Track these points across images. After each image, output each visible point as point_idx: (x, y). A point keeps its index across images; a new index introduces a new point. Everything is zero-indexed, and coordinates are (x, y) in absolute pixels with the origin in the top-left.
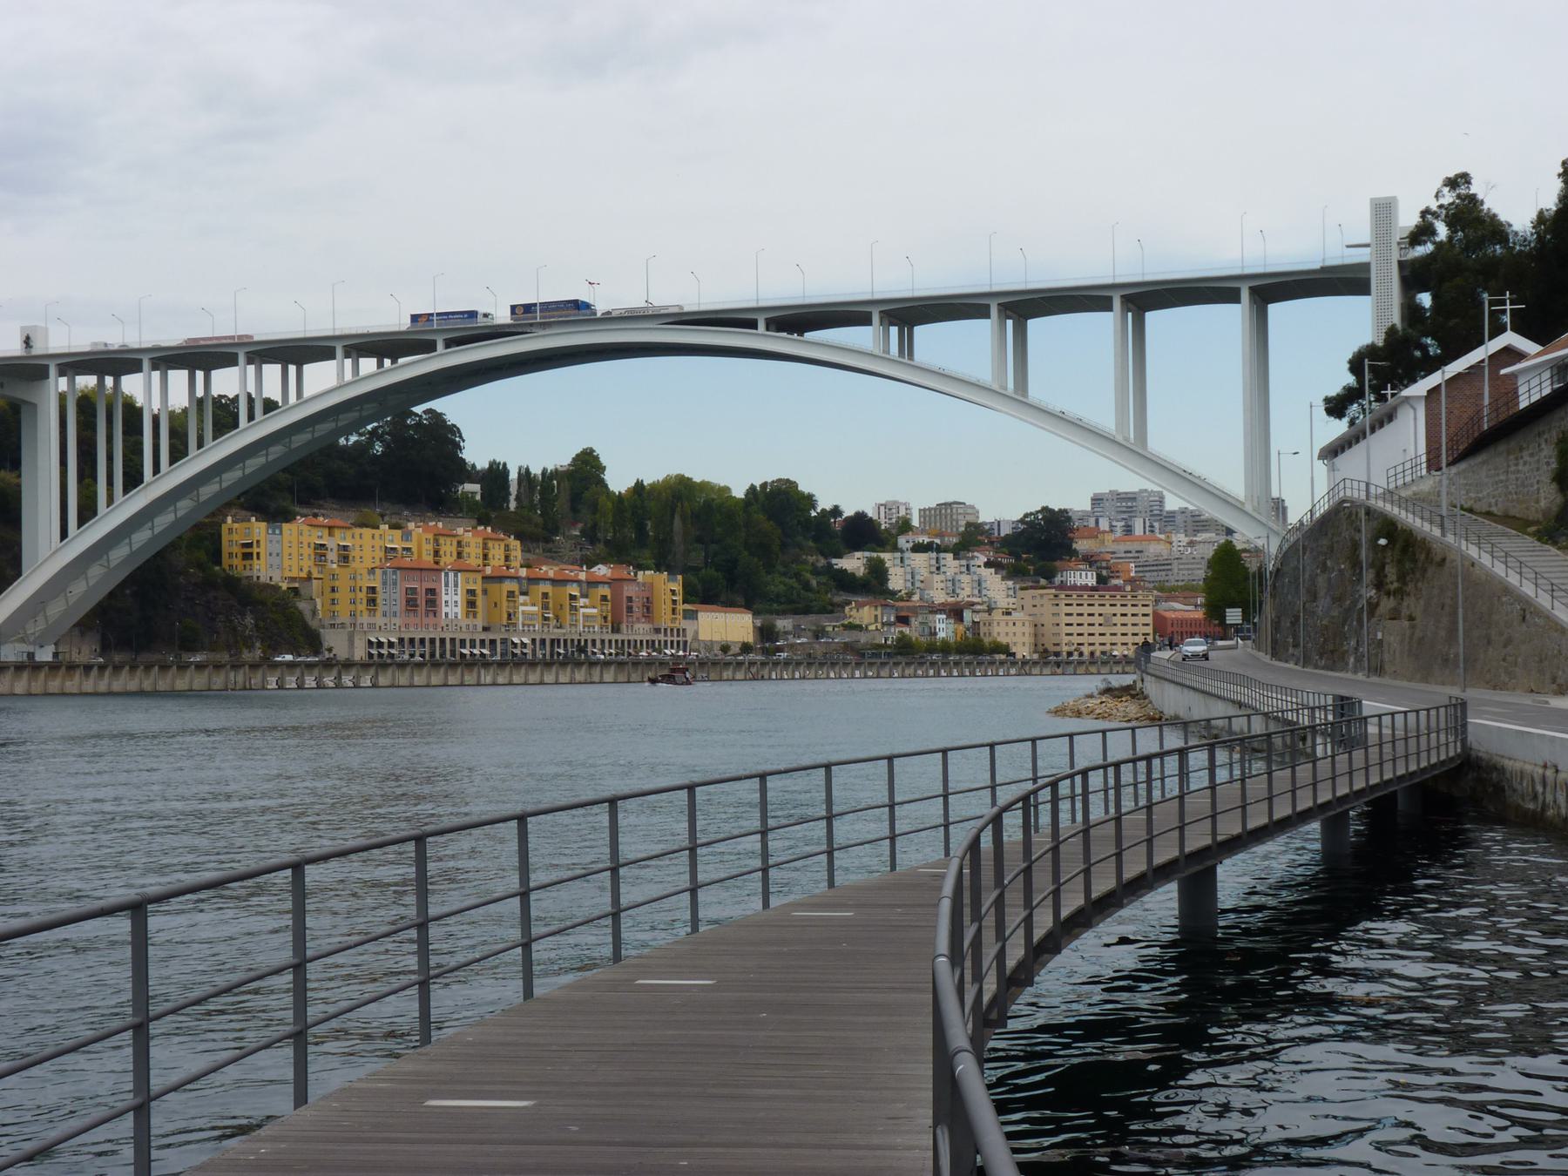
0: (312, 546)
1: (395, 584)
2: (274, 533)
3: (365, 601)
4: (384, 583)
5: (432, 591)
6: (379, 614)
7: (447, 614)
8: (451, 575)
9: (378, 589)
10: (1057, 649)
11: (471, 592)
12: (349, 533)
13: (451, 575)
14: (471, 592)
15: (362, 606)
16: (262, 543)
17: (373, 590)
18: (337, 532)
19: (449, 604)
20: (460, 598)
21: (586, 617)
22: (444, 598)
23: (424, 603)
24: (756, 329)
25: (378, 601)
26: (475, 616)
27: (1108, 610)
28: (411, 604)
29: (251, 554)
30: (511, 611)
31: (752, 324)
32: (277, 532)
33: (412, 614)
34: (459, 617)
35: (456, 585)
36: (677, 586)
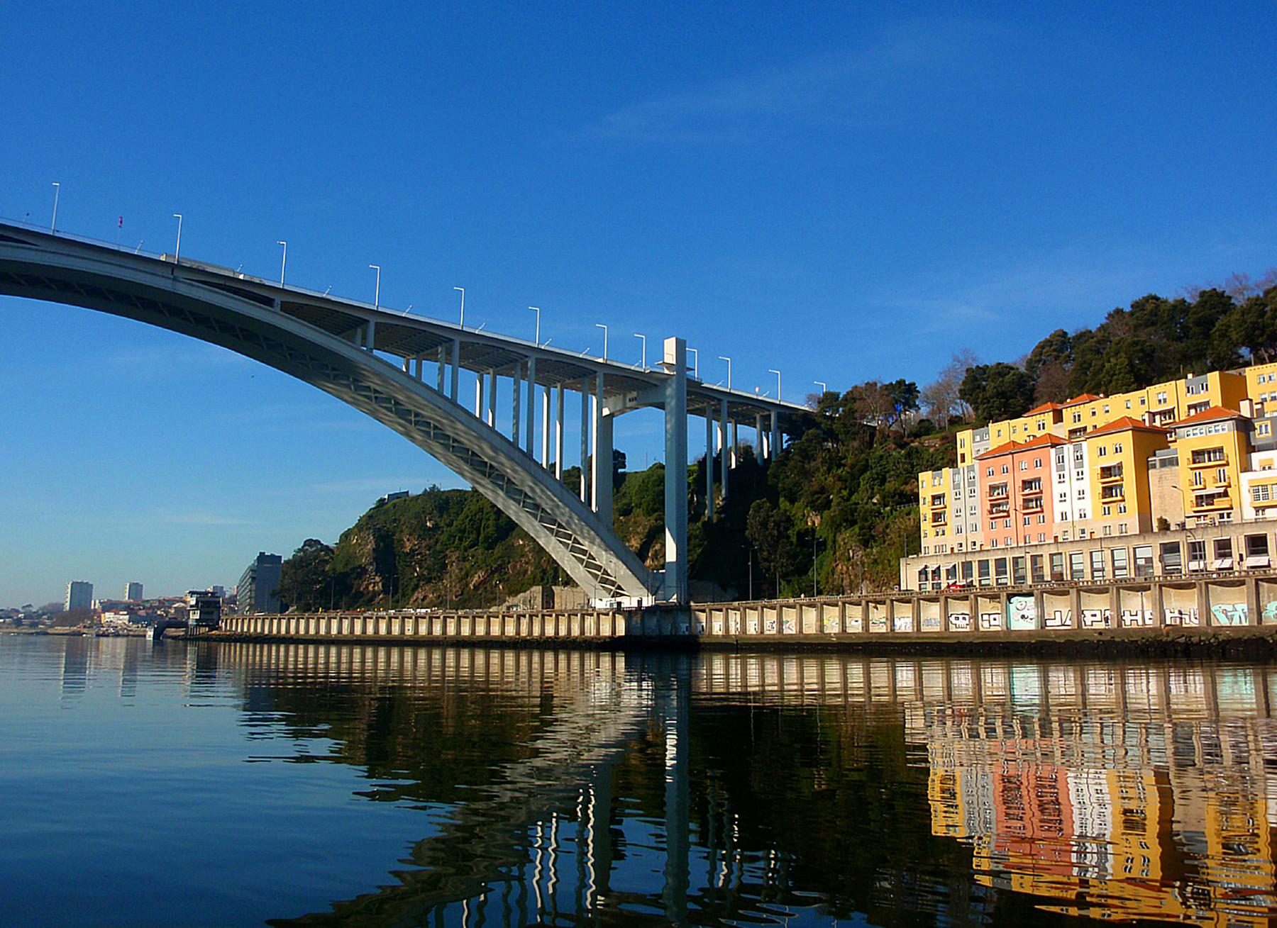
7: (1064, 516)
12: (1085, 410)
18: (1067, 414)
20: (1092, 484)
22: (1058, 489)
28: (997, 508)
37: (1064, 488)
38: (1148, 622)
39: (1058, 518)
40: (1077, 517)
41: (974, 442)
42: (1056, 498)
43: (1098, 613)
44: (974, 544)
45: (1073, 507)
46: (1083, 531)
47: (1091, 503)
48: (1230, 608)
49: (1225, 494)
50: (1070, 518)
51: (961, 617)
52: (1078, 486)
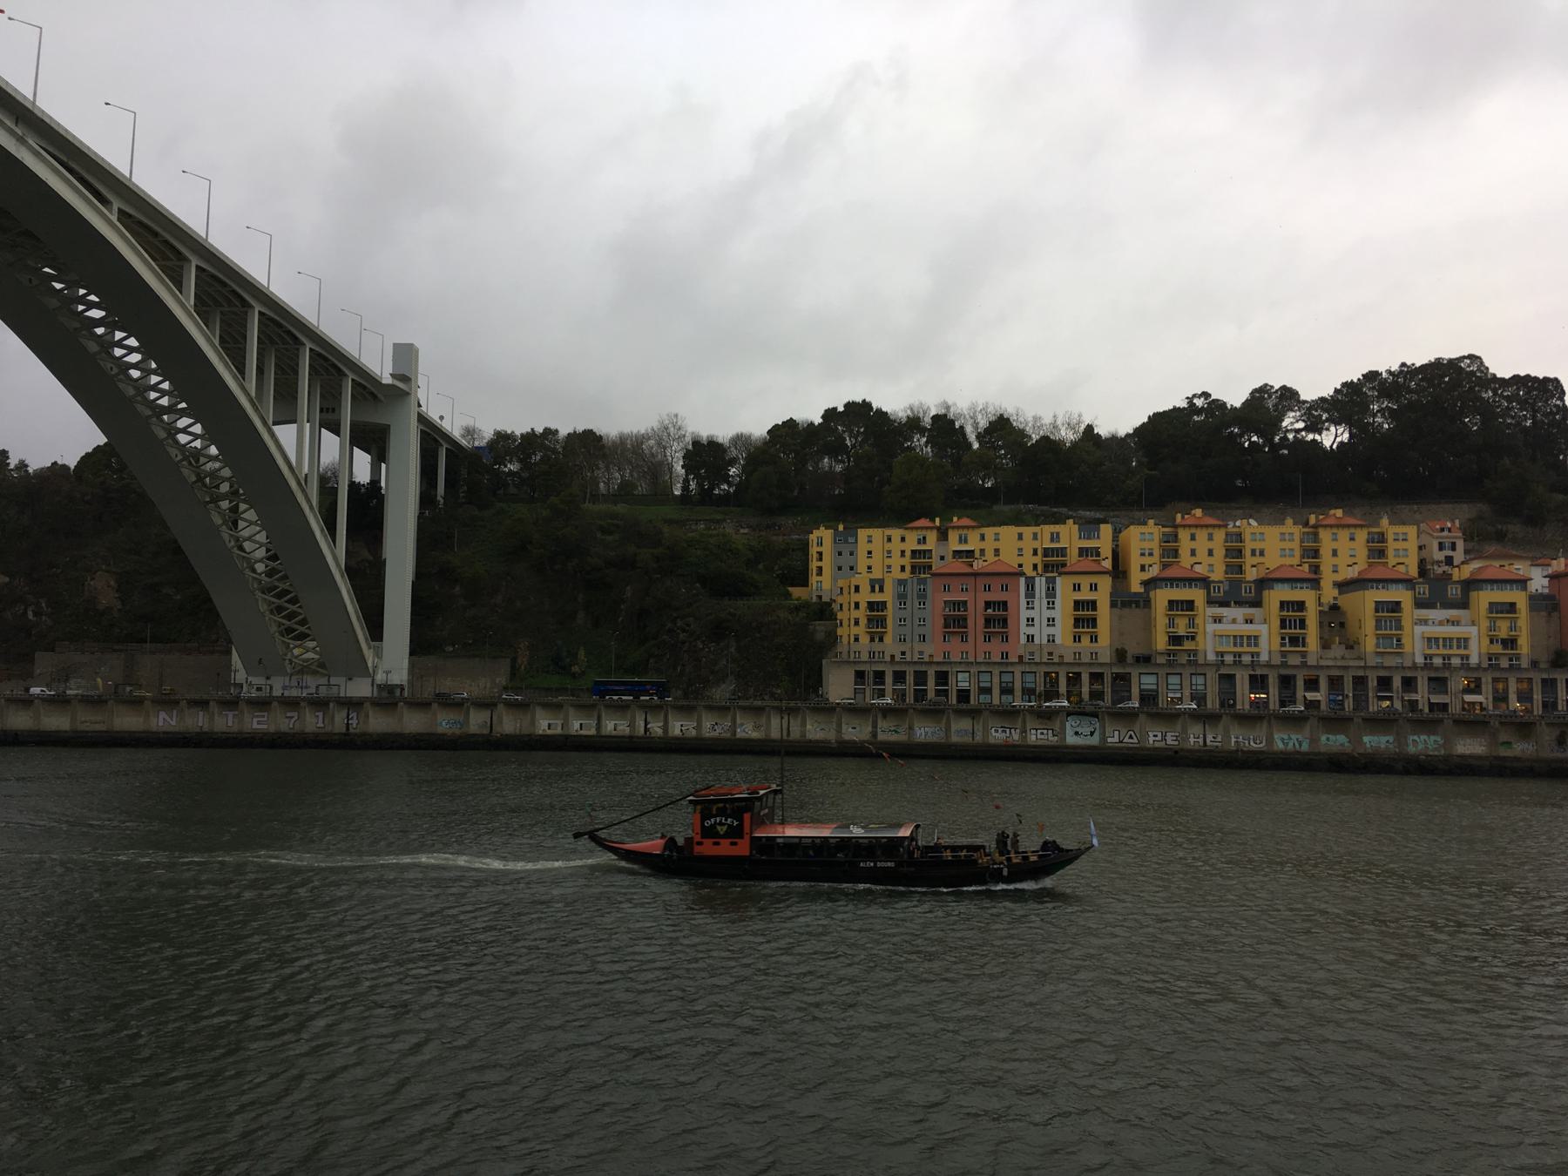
0: (908, 554)
1: (922, 596)
2: (846, 542)
3: (863, 622)
4: (902, 598)
6: (888, 639)
7: (1030, 638)
8: (1040, 584)
9: (889, 606)
11: (1093, 605)
13: (1040, 584)
18: (953, 536)
19: (1036, 621)
21: (1431, 641)
22: (1024, 614)
23: (981, 622)
25: (889, 622)
26: (1094, 639)
28: (955, 622)
30: (1181, 632)
32: (851, 540)
33: (956, 640)
34: (1058, 641)
35: (1051, 593)
37: (1031, 614)
38: (1208, 742)
39: (1023, 640)
40: (1045, 641)
41: (835, 542)
42: (1023, 622)
43: (1160, 734)
44: (921, 653)
45: (1041, 633)
46: (1050, 654)
47: (1063, 632)
48: (1286, 737)
49: (1193, 638)
50: (1037, 640)
51: (1000, 730)
52: (1048, 614)
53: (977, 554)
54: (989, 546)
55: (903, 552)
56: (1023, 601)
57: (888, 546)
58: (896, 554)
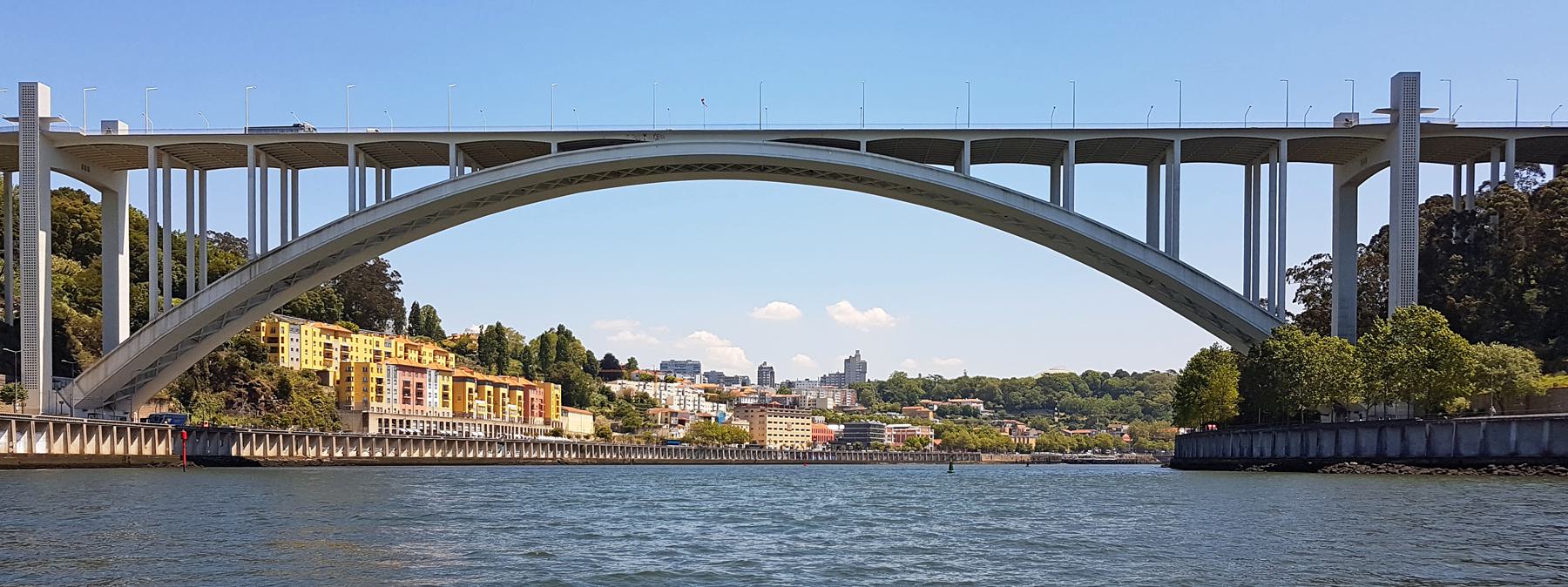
0: (322, 345)
5: (419, 385)
10: (763, 444)
14: (445, 387)
15: (373, 394)
16: (285, 340)
17: (380, 381)
20: (439, 391)
22: (429, 390)
24: (859, 150)
25: (384, 390)
27: (789, 420)
29: (278, 348)
31: (856, 146)
35: (436, 381)
36: (556, 391)
42: (428, 395)
47: (439, 400)
52: (435, 391)
53: (350, 348)
54: (354, 344)
55: (320, 343)
56: (428, 383)
57: (315, 339)
58: (317, 344)
